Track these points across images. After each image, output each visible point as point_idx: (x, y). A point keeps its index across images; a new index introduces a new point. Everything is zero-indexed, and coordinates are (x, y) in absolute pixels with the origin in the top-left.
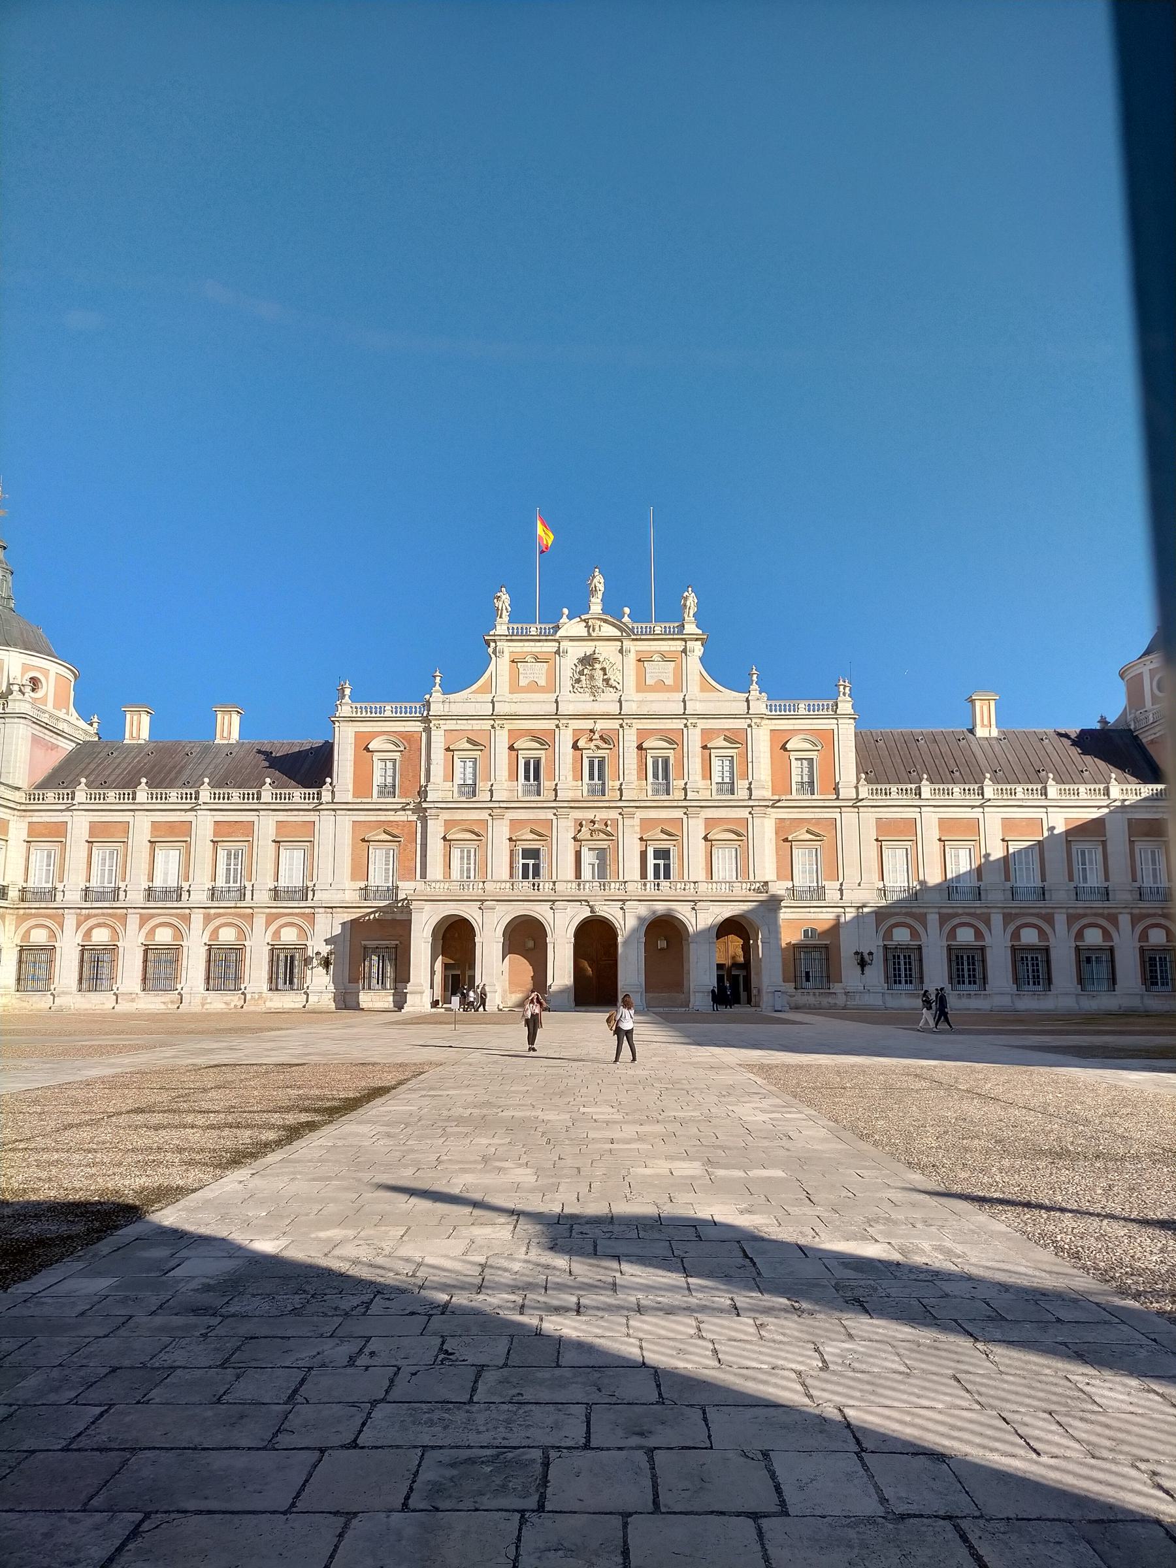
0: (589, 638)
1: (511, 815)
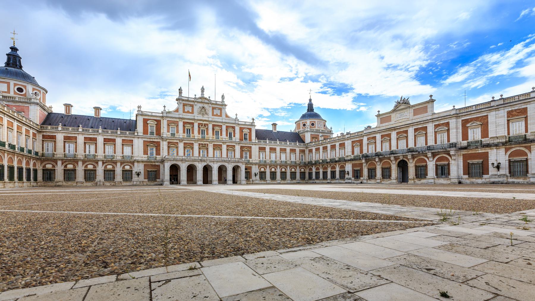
1: (184, 142)
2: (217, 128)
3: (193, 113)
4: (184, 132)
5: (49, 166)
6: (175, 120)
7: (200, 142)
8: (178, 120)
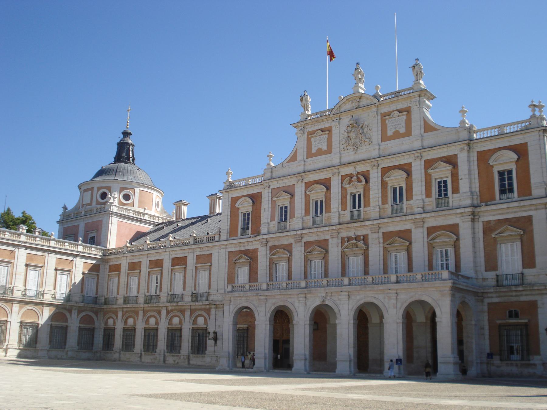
3: (331, 152)
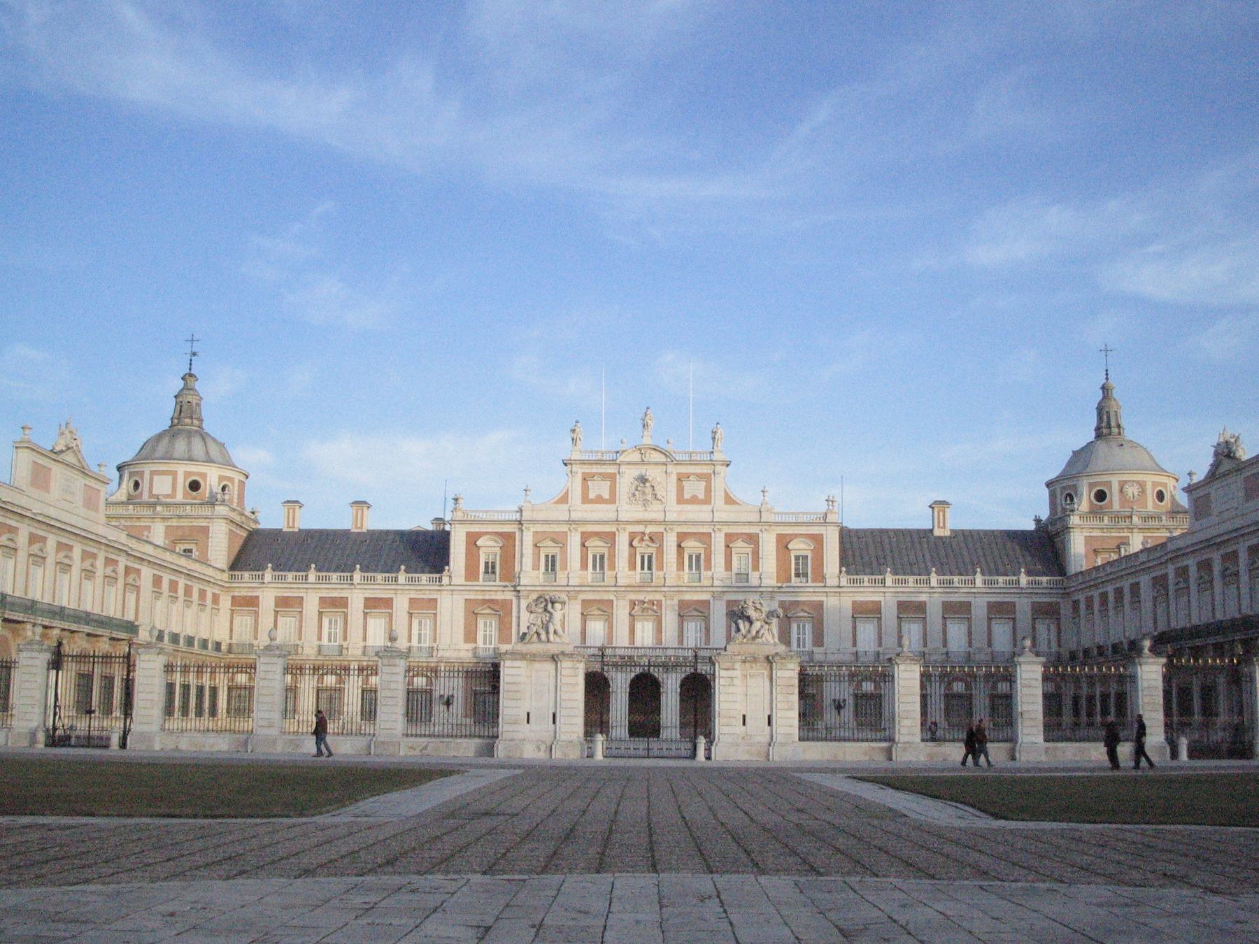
0: (643, 462)
2: (692, 546)
4: (584, 566)
5: (241, 679)
6: (556, 528)
7: (633, 597)
8: (564, 528)
